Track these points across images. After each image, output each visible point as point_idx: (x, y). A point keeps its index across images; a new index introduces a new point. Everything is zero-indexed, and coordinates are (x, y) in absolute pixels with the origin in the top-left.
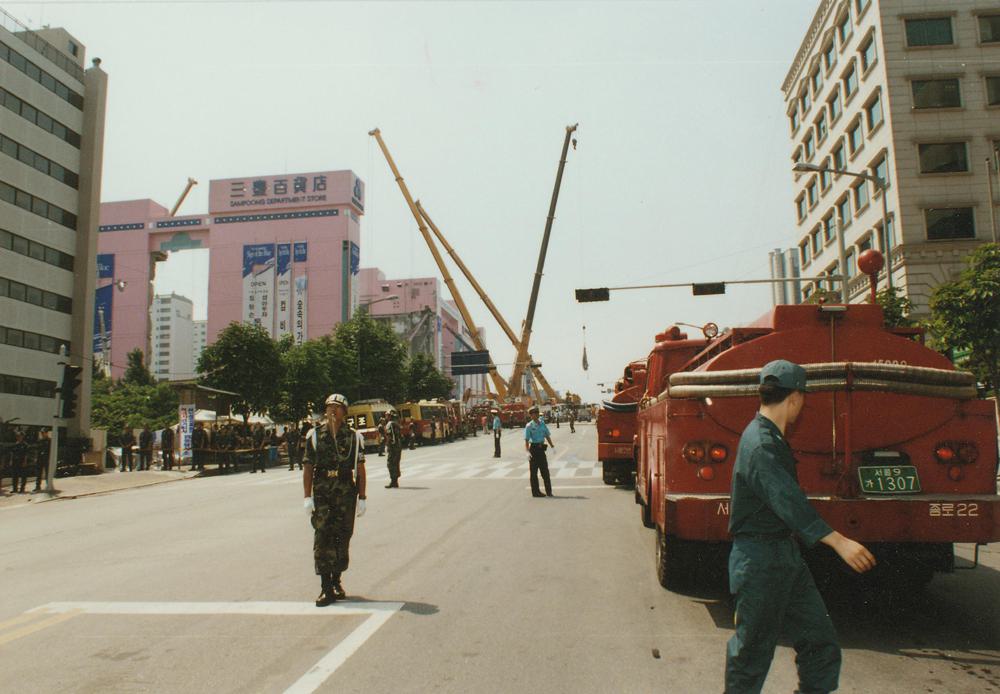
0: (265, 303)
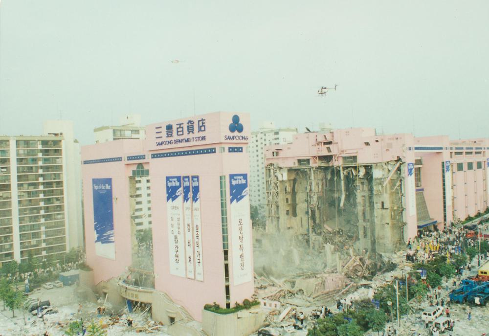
0: (179, 224)
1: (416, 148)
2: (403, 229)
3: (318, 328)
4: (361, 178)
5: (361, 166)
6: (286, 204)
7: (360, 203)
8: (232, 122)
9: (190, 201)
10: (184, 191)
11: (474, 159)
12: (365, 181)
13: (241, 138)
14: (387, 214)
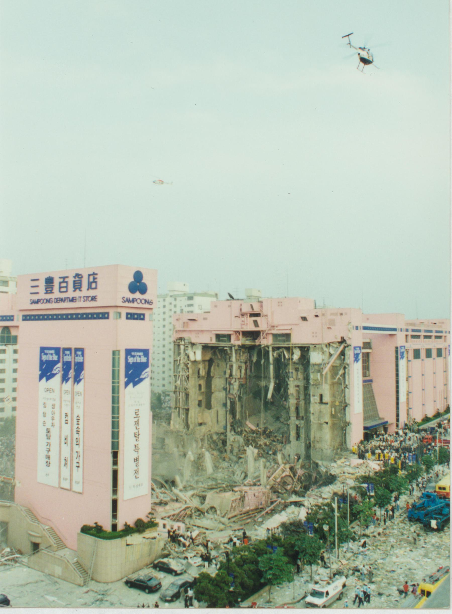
0: (53, 413)
1: (365, 328)
2: (345, 430)
3: (233, 560)
4: (295, 363)
5: (295, 347)
6: (198, 392)
7: (292, 394)
8: (132, 280)
9: (70, 382)
10: (63, 367)
11: (433, 344)
12: (300, 367)
13: (143, 301)
14: (327, 410)
